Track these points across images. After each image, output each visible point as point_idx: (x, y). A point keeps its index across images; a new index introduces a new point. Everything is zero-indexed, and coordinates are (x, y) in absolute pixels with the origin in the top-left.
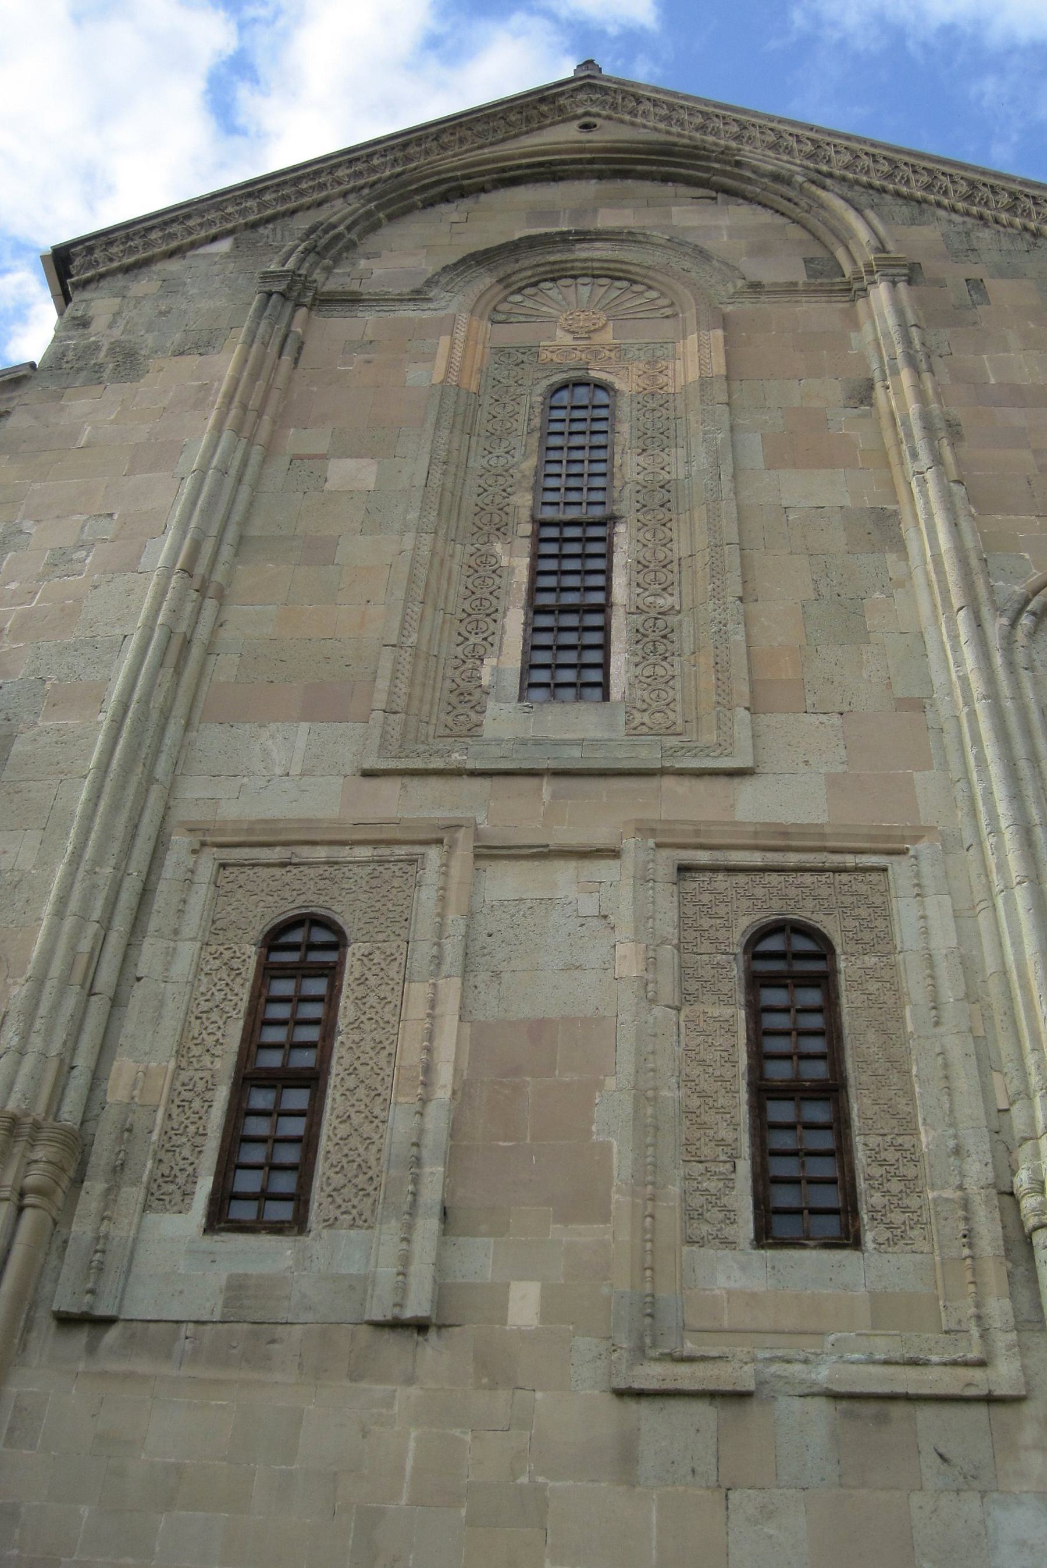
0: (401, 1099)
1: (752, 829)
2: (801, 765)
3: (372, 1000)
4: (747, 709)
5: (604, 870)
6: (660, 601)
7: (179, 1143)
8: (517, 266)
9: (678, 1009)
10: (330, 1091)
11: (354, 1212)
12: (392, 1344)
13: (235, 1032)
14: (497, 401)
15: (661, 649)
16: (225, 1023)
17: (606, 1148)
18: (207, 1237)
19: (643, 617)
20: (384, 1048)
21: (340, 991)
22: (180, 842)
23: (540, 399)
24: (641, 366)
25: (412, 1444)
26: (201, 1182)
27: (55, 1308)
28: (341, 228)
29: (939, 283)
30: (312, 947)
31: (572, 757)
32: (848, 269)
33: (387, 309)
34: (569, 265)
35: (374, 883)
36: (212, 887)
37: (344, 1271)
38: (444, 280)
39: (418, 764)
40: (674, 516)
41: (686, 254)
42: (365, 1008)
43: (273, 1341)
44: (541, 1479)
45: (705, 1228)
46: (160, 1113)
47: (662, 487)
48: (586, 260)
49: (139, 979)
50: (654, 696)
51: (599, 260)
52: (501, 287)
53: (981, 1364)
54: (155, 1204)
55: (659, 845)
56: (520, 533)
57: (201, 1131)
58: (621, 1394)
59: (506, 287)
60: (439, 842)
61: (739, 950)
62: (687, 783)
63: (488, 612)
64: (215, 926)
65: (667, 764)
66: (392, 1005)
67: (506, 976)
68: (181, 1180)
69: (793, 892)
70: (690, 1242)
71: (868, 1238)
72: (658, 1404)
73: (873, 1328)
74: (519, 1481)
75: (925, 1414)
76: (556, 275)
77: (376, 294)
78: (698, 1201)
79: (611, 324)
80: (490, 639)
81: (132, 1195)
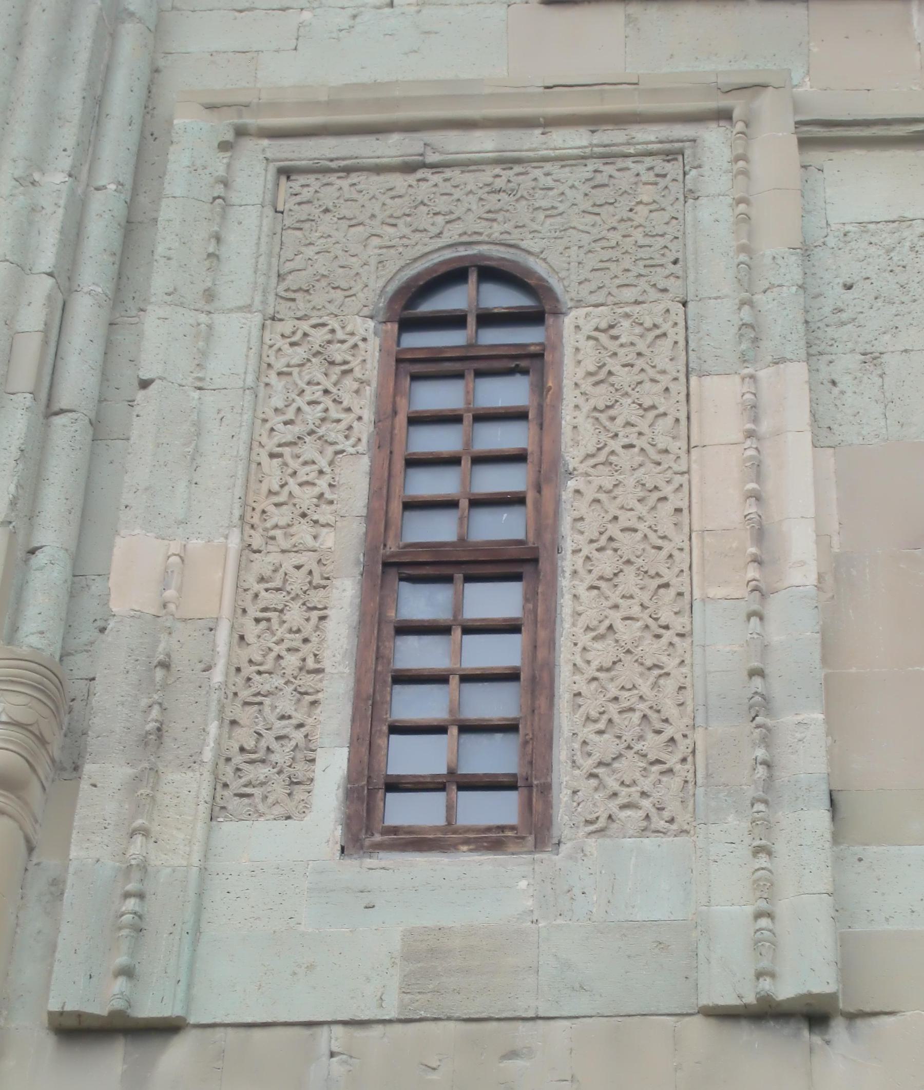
0: (714, 592)
3: (626, 411)
10: (565, 582)
11: (646, 803)
16: (331, 463)
20: (664, 499)
21: (559, 397)
26: (321, 757)
27: (54, 1006)
30: (488, 319)
35: (601, 195)
36: (269, 211)
42: (614, 427)
43: (512, 1054)
46: (223, 634)
49: (145, 384)
54: (235, 804)
57: (311, 663)
60: (724, 115)
64: (283, 286)
66: (669, 420)
67: (892, 362)
68: (281, 755)
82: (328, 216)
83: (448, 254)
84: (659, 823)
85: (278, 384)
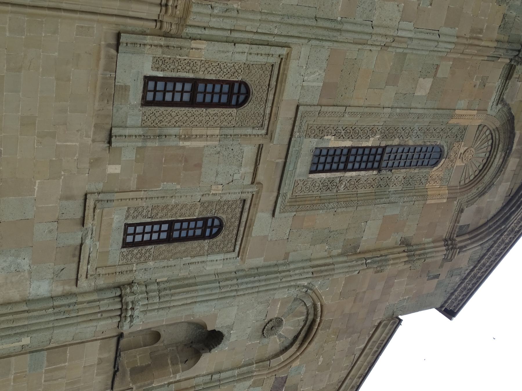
0: (181, 130)
1: (253, 218)
2: (273, 229)
3: (216, 118)
4: (295, 215)
5: (248, 180)
7: (176, 64)
9: (199, 201)
12: (104, 135)
13: (213, 77)
15: (324, 188)
16: (215, 73)
17: (159, 187)
18: (143, 77)
19: (338, 182)
22: (284, 51)
24: (441, 175)
25: (74, 144)
26: (162, 72)
29: (441, 266)
31: (290, 167)
32: (458, 239)
34: (496, 150)
37: (128, 119)
39: (297, 123)
40: (374, 189)
41: (485, 189)
44: (62, 177)
45: (132, 212)
46: (186, 58)
48: (495, 156)
50: (308, 186)
51: (494, 160)
53: (87, 277)
54: (156, 59)
55: (253, 195)
57: (179, 71)
58: (86, 195)
59: (494, 130)
60: (267, 134)
61: (216, 215)
65: (280, 195)
67: (218, 155)
68: (163, 66)
69: (231, 228)
70: (129, 208)
71: (125, 249)
72: (83, 205)
73: (99, 252)
74: (62, 172)
75: (75, 266)
76: (494, 145)
77: (507, 86)
78: (140, 210)
80: (342, 137)
81: (159, 52)
82: (263, 72)
83: (251, 91)
84: (143, 122)
85: (232, 65)
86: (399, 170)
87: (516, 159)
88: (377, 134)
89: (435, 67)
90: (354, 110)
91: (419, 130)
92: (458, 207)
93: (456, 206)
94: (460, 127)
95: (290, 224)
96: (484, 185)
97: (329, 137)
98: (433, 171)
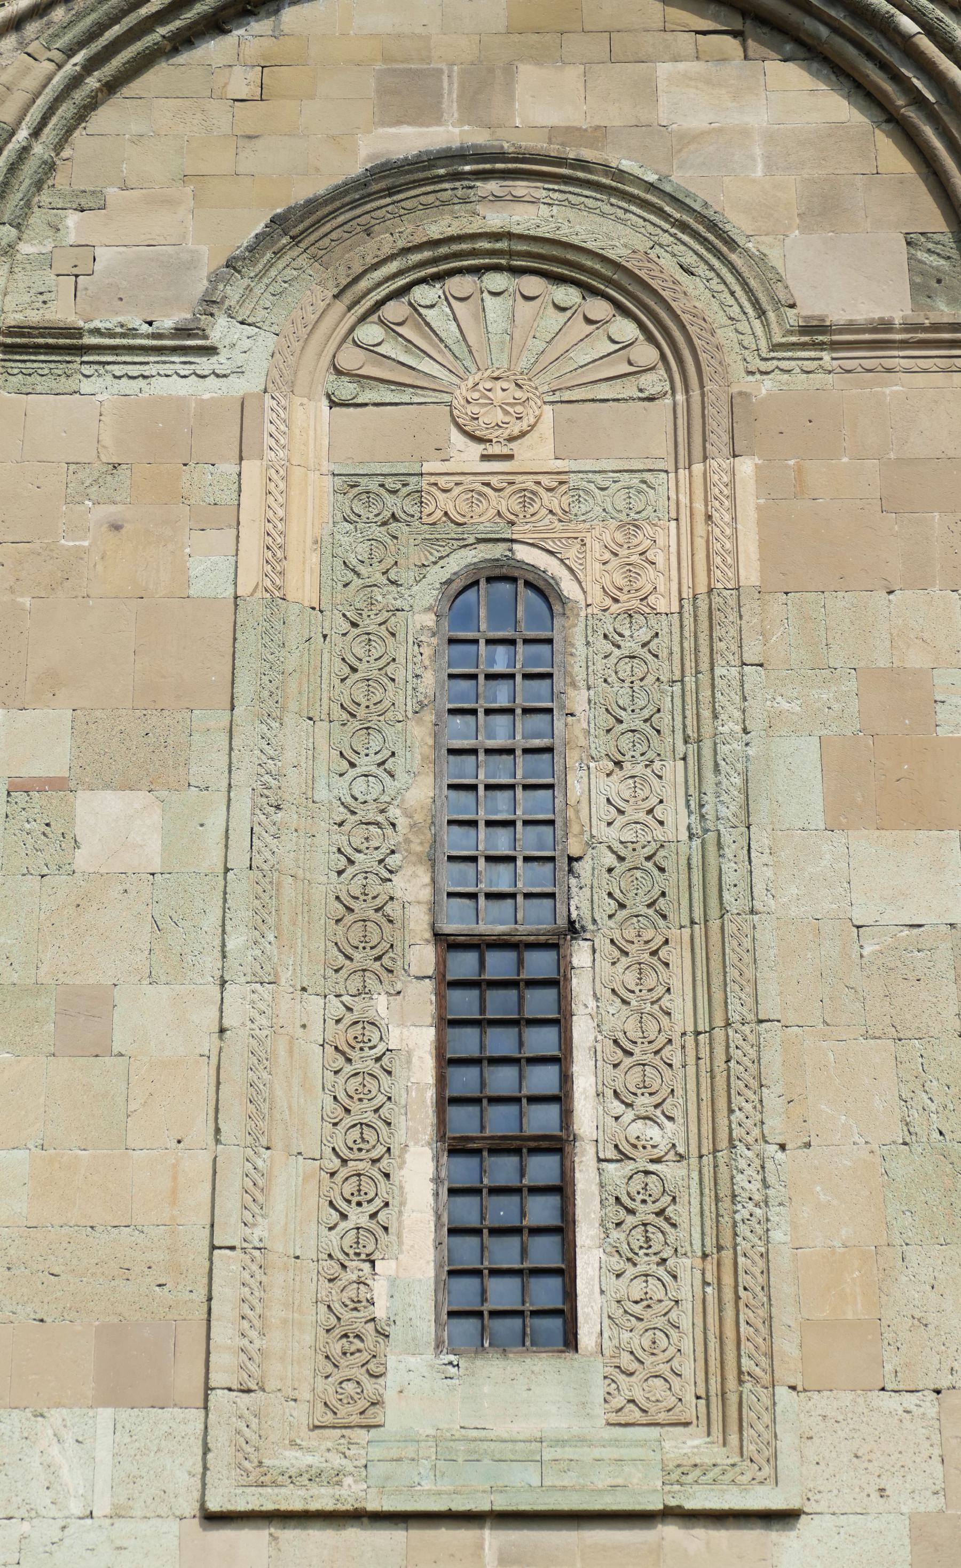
2: (875, 1496)
6: (653, 1132)
8: (372, 249)
14: (355, 625)
23: (429, 620)
24: (607, 538)
28: (23, 134)
33: (134, 370)
38: (233, 293)
39: (293, 1500)
47: (648, 858)
50: (646, 1343)
52: (340, 307)
56: (414, 970)
62: (701, 1535)
63: (375, 1154)
65: (673, 1503)
77: (111, 334)
79: (548, 409)
80: (381, 1217)
86: (571, 813)
87: (519, 89)
88: (371, 1014)
89: (20, 797)
90: (230, 1201)
91: (353, 765)
92: (784, 365)
93: (786, 376)
94: (339, 517)
95: (846, 1398)
96: (666, 239)
97: (380, 1289)
98: (579, 596)
